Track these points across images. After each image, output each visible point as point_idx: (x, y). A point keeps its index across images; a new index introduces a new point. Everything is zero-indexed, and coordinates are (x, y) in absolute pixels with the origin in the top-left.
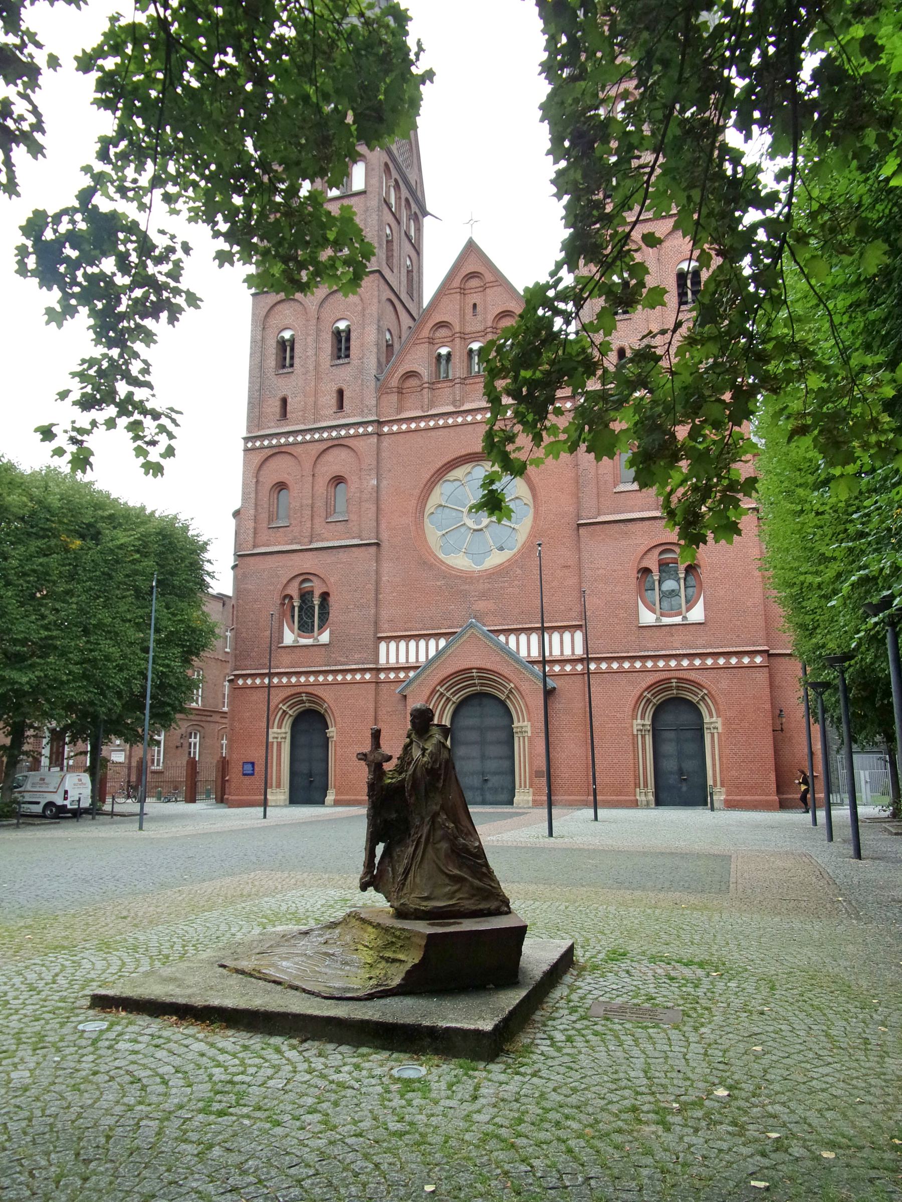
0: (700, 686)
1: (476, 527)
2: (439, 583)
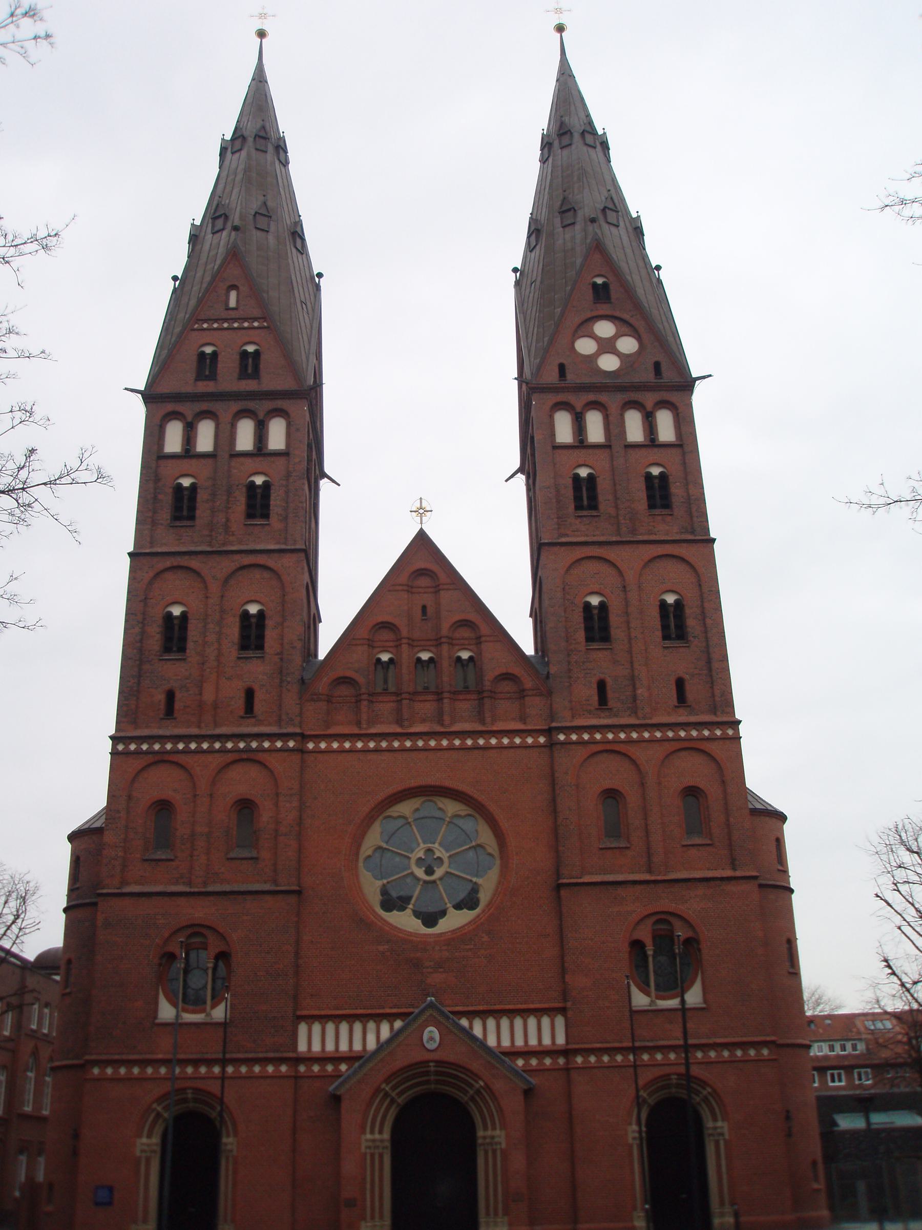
0: (704, 1084)
1: (427, 878)
2: (381, 948)
